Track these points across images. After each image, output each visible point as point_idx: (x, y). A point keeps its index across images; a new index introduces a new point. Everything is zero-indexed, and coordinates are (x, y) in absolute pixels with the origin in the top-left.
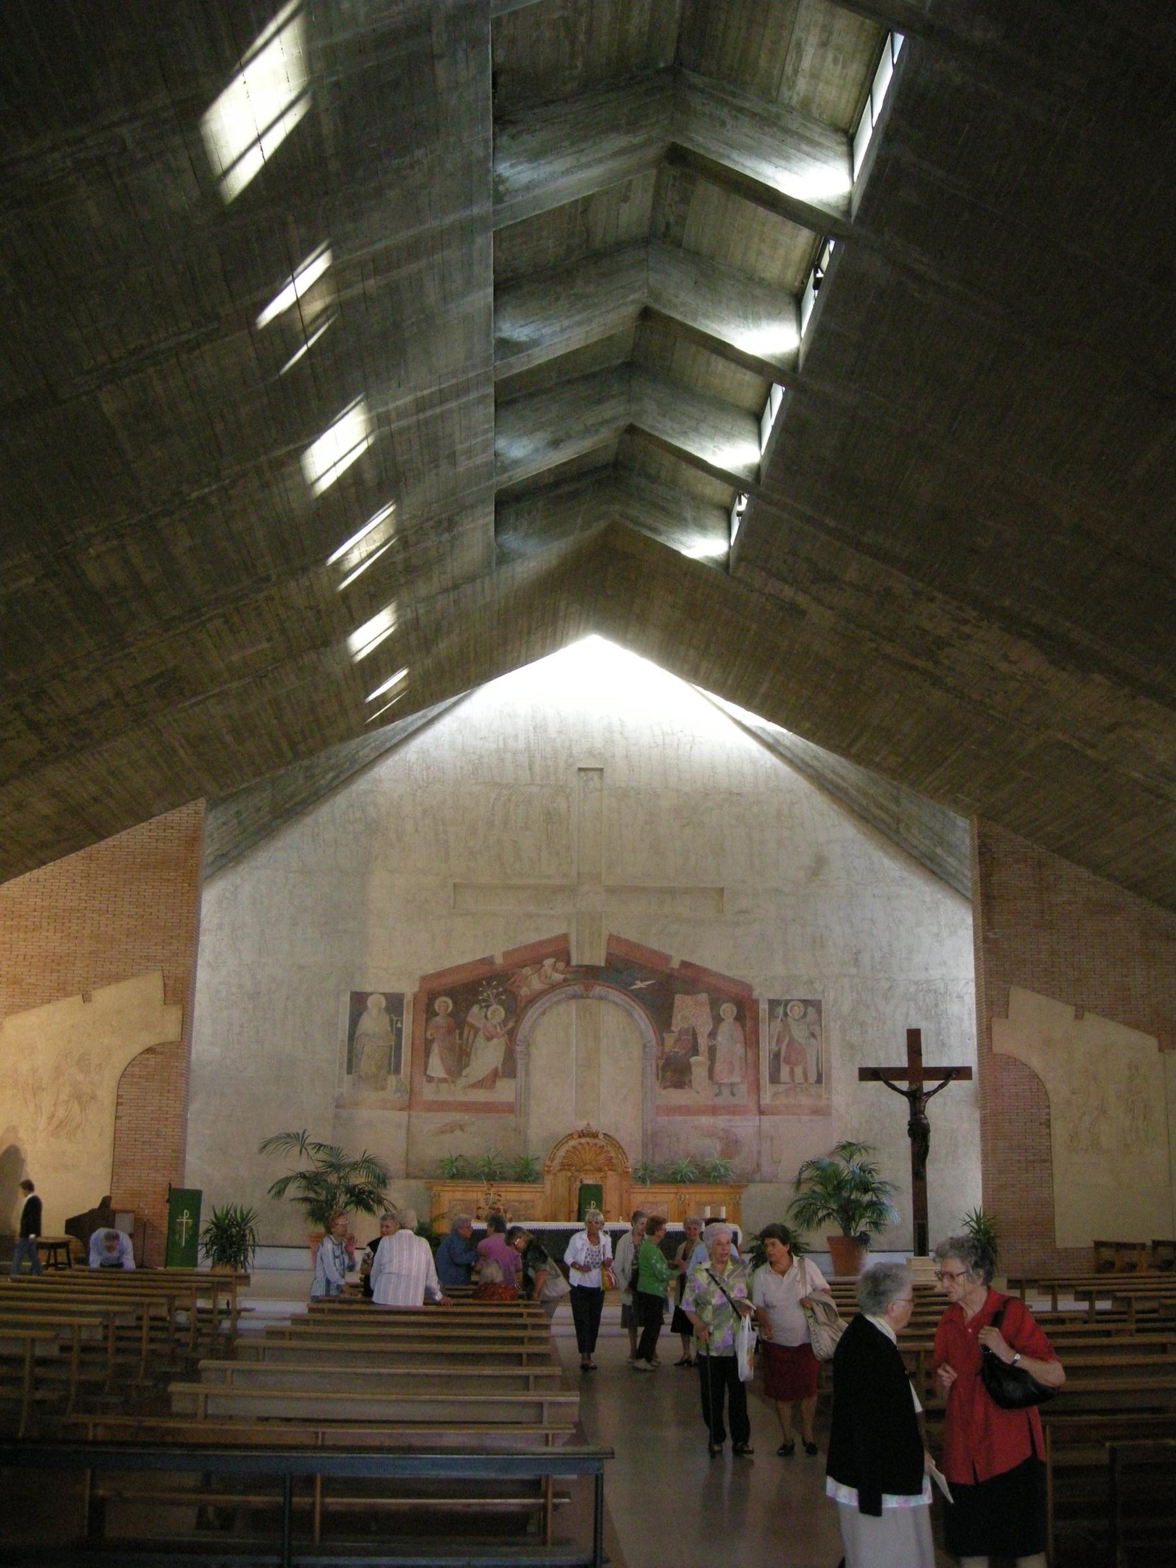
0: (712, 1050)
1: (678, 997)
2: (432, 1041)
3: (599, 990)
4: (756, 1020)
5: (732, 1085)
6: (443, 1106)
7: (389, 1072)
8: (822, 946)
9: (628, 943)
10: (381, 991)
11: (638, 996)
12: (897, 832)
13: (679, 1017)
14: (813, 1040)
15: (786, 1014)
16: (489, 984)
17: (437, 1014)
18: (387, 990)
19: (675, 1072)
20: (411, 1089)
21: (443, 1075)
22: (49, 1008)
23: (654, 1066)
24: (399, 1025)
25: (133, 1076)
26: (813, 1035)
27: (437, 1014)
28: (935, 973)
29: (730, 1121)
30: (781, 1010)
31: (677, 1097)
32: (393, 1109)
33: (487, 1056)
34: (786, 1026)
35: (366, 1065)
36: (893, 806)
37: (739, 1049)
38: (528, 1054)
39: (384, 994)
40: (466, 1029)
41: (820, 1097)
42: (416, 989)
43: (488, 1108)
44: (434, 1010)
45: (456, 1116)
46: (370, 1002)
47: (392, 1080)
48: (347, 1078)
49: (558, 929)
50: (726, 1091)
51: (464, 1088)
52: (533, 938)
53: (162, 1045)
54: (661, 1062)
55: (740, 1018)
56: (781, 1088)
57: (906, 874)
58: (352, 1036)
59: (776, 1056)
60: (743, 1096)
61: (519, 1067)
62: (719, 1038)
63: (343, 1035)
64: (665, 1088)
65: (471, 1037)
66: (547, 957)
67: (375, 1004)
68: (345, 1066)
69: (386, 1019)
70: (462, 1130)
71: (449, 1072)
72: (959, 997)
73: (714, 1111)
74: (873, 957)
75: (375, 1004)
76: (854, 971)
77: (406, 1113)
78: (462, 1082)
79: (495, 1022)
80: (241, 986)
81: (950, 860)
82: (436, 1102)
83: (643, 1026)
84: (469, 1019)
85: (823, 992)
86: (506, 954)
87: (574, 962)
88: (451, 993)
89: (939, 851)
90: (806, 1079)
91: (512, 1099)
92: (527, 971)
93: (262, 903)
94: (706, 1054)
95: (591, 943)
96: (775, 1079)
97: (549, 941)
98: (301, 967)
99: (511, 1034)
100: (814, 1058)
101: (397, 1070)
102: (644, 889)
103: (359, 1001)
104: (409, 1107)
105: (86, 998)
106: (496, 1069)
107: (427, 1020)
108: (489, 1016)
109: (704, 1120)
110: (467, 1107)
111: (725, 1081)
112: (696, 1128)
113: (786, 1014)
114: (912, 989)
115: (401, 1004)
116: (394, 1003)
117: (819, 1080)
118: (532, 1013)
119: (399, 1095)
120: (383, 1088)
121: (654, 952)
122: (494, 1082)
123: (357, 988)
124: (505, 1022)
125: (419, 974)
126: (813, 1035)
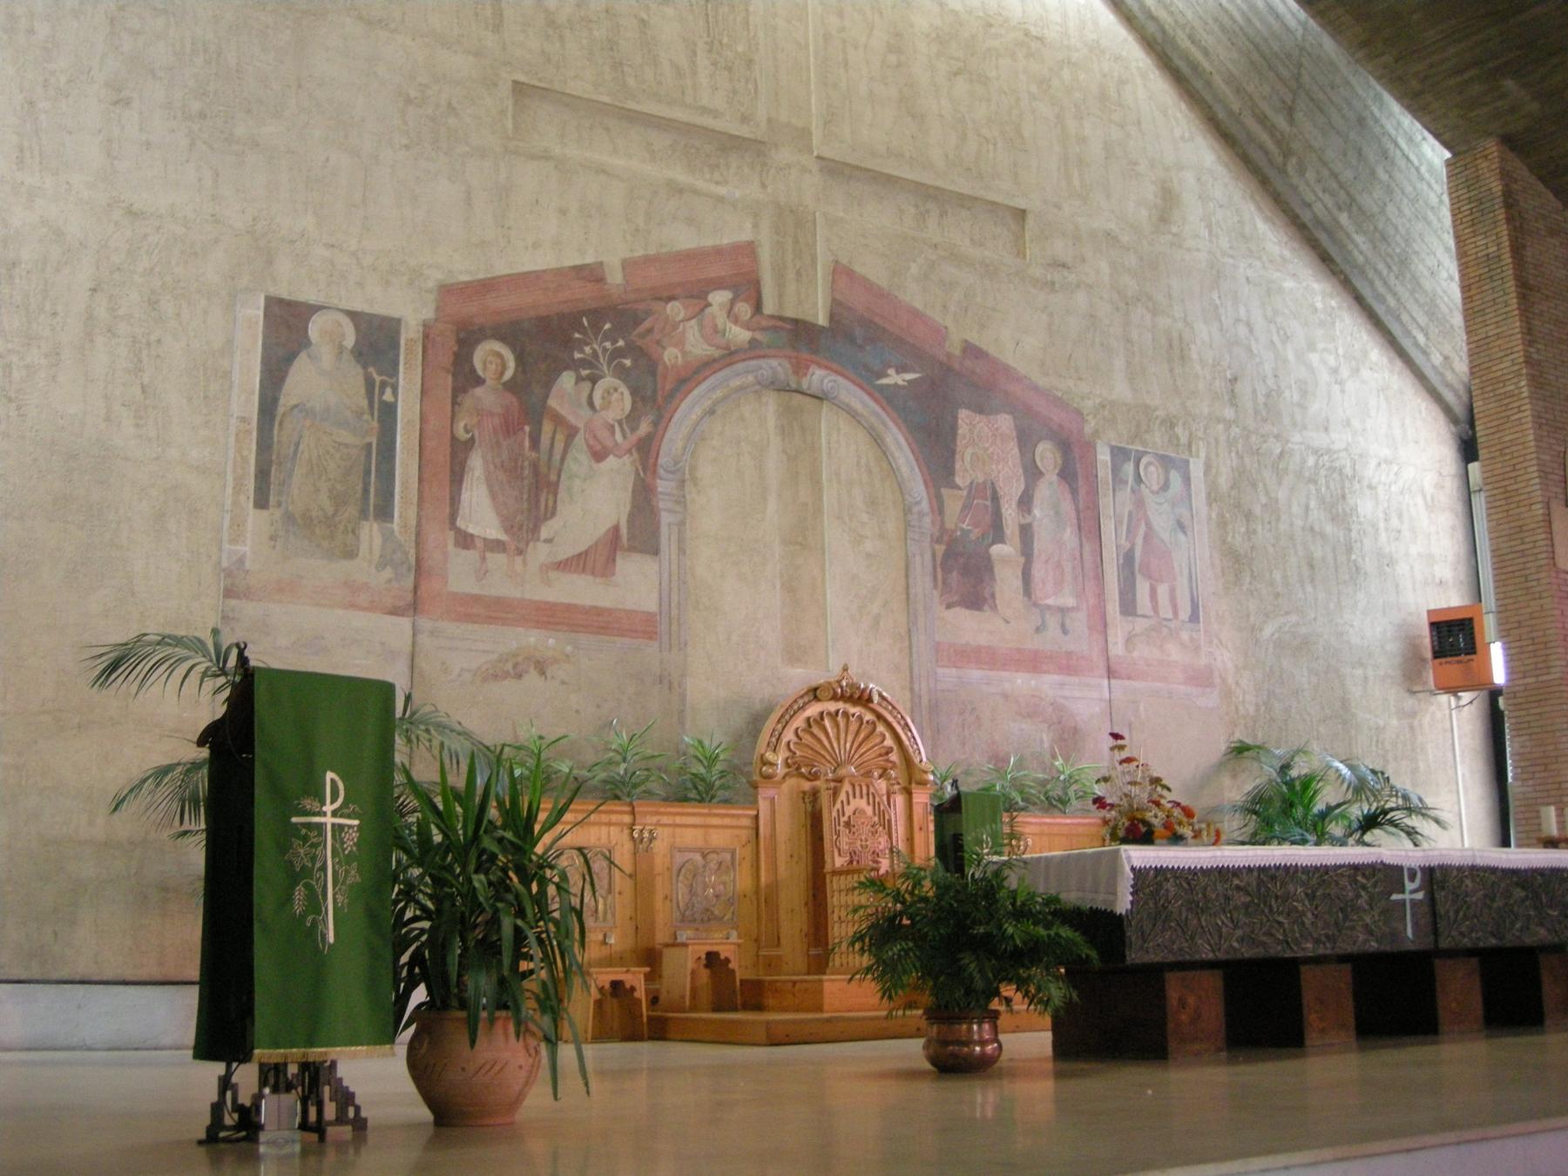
0: (1026, 532)
1: (964, 414)
2: (469, 444)
3: (818, 377)
4: (1092, 479)
5: (1063, 611)
6: (496, 611)
7: (364, 513)
8: (1182, 358)
9: (867, 285)
11: (888, 398)
12: (1283, 171)
13: (968, 458)
14: (1181, 537)
15: (1138, 479)
16: (596, 327)
17: (479, 381)
18: (358, 307)
19: (965, 573)
20: (418, 560)
21: (494, 532)
23: (928, 556)
24: (388, 396)
26: (1181, 526)
27: (479, 381)
28: (1339, 438)
29: (1062, 685)
30: (1129, 468)
31: (968, 627)
32: (372, 607)
33: (595, 498)
34: (1140, 503)
35: (301, 489)
36: (1281, 122)
37: (1069, 535)
38: (681, 501)
39: (354, 316)
40: (547, 427)
41: (1197, 649)
42: (429, 313)
43: (600, 622)
44: (473, 370)
45: (532, 639)
46: (315, 329)
47: (370, 532)
48: (256, 521)
49: (734, 231)
50: (1053, 622)
51: (546, 568)
52: (684, 239)
54: (941, 549)
55: (1067, 474)
56: (1140, 625)
57: (1287, 253)
59: (1128, 560)
60: (1081, 641)
61: (664, 530)
62: (1037, 512)
63: (245, 401)
64: (949, 607)
65: (559, 446)
66: (719, 284)
67: (328, 335)
69: (355, 377)
70: (542, 673)
71: (509, 528)
72: (1370, 487)
73: (1034, 662)
74: (1254, 392)
75: (328, 335)
76: (1229, 413)
77: (405, 623)
78: (540, 553)
79: (612, 415)
81: (1359, 239)
82: (477, 599)
83: (905, 470)
84: (552, 402)
85: (1190, 446)
86: (628, 265)
87: (769, 307)
88: (509, 332)
89: (1344, 218)
90: (1175, 613)
91: (651, 606)
92: (675, 309)
93: (31, 31)
94: (1017, 540)
95: (798, 273)
96: (1128, 607)
97: (718, 252)
98: (133, 214)
99: (646, 450)
100: (1186, 572)
101: (384, 512)
102: (890, 180)
103: (287, 324)
104: (414, 606)
106: (616, 529)
107: (458, 391)
108: (597, 401)
109: (1021, 682)
110: (550, 616)
111: (1050, 601)
112: (1005, 696)
113: (1138, 479)
114: (1311, 461)
115: (395, 345)
116: (376, 342)
117: (1194, 617)
118: (688, 411)
119: (388, 573)
120: (350, 554)
121: (916, 314)
122: (611, 560)
123: (285, 296)
124: (632, 419)
125: (435, 277)
126: (1181, 526)
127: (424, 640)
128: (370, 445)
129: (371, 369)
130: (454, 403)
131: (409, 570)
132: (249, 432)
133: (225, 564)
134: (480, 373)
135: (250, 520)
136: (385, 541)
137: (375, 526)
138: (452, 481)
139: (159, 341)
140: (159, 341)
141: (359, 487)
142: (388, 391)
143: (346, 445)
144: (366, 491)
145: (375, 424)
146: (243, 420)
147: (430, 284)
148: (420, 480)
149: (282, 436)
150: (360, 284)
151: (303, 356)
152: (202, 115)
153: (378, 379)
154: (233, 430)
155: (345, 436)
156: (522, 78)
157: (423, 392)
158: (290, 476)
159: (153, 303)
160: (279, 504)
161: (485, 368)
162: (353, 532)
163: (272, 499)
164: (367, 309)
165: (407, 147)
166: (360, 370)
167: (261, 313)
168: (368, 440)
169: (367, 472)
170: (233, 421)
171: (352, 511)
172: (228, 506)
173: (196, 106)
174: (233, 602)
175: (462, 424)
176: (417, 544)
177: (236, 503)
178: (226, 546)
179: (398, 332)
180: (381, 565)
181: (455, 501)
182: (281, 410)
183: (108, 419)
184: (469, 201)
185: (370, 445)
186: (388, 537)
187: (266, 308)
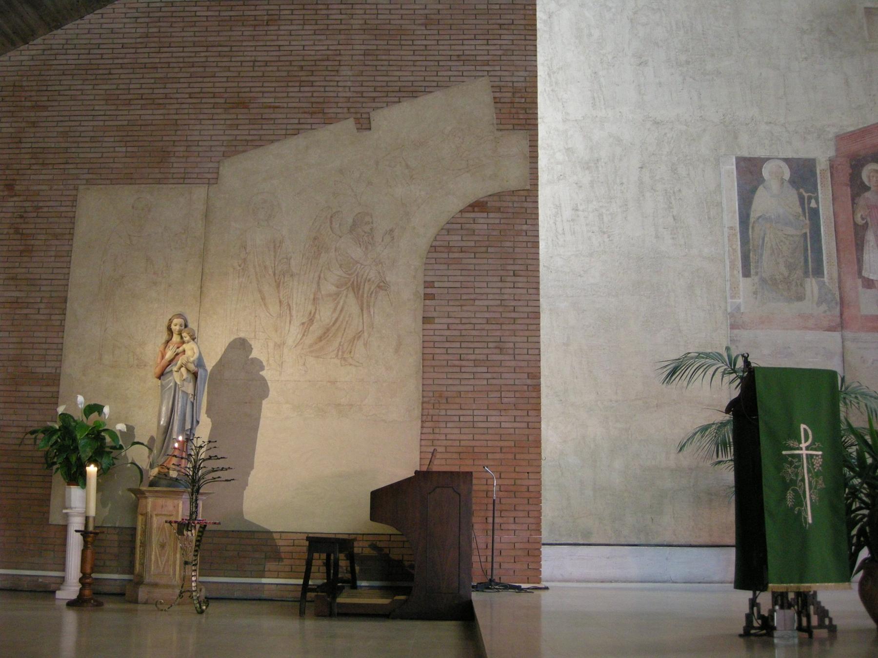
2: (865, 227)
7: (806, 274)
10: (781, 156)
17: (867, 189)
18: (790, 155)
20: (841, 298)
22: (300, 141)
24: (813, 204)
25: (449, 248)
27: (867, 189)
32: (817, 327)
35: (768, 264)
39: (786, 160)
42: (831, 153)
44: (862, 183)
46: (765, 173)
47: (812, 285)
48: (745, 284)
53: (499, 195)
58: (744, 219)
63: (731, 217)
68: (739, 264)
69: (792, 196)
77: (837, 335)
80: (569, 151)
93: (590, 35)
98: (656, 123)
101: (818, 271)
103: (750, 171)
104: (841, 325)
105: (364, 124)
116: (802, 174)
119: (824, 307)
120: (800, 298)
123: (746, 154)
125: (832, 131)
127: (848, 344)
128: (806, 234)
129: (801, 190)
130: (853, 203)
131: (837, 303)
132: (735, 235)
133: (729, 310)
134: (867, 183)
135: (741, 285)
136: (820, 289)
137: (814, 281)
138: (857, 250)
139: (680, 190)
140: (680, 190)
141: (802, 260)
142: (813, 201)
143: (792, 236)
144: (806, 261)
145: (807, 222)
146: (731, 228)
147: (831, 136)
148: (837, 250)
149: (754, 234)
150: (789, 143)
151: (761, 188)
152: (688, 63)
153: (806, 195)
154: (726, 235)
155: (790, 231)
156: (869, 5)
157: (834, 199)
158: (762, 255)
159: (674, 170)
160: (757, 273)
161: (870, 181)
162: (801, 285)
163: (753, 272)
164: (795, 156)
165: (806, 59)
166: (795, 192)
167: (734, 167)
168: (804, 231)
169: (806, 250)
170: (726, 229)
171: (799, 273)
172: (728, 277)
173: (683, 58)
174: (736, 331)
175: (859, 215)
176: (840, 288)
177: (732, 275)
178: (729, 300)
179: (815, 166)
180: (819, 303)
181: (860, 261)
182: (752, 220)
183: (657, 237)
184: (847, 83)
185: (806, 234)
186: (822, 285)
187: (737, 164)
